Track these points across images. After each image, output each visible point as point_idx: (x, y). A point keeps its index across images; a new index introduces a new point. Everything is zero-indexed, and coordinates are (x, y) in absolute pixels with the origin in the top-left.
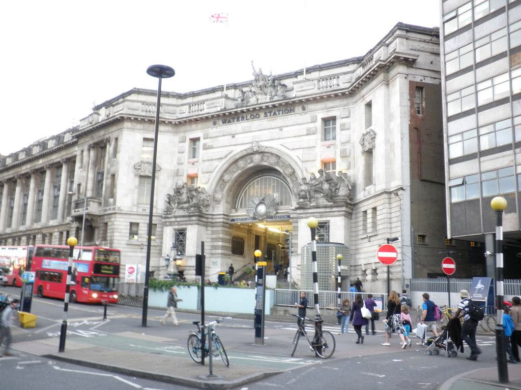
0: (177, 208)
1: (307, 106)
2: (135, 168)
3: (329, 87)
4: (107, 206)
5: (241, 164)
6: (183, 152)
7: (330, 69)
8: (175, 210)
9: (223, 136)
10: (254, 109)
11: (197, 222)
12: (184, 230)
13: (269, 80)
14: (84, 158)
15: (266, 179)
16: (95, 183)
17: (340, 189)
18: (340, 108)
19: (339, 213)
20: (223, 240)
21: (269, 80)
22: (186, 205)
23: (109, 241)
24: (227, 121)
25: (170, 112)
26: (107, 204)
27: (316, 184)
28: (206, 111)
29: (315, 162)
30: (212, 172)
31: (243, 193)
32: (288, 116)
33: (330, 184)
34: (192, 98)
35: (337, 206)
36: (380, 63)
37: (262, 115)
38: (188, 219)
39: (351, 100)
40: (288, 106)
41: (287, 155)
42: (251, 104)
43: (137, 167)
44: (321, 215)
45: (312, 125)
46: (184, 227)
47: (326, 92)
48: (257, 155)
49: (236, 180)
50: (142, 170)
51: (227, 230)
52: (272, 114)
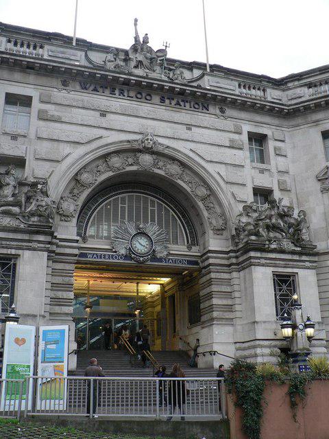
5: (116, 161)
9: (84, 108)
12: (10, 260)
15: (138, 199)
22: (16, 209)
24: (92, 88)
30: (58, 161)
31: (95, 213)
32: (200, 114)
35: (306, 254)
37: (156, 99)
38: (26, 237)
40: (200, 100)
41: (203, 167)
45: (236, 137)
46: (13, 252)
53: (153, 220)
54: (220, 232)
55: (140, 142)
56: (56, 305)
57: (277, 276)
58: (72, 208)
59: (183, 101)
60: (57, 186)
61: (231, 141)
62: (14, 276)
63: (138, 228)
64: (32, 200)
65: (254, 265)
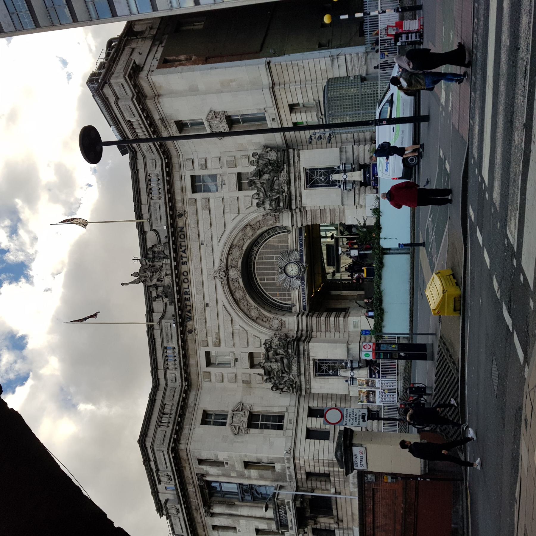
0: (289, 373)
1: (177, 212)
2: (238, 433)
3: (160, 195)
4: (285, 474)
5: (239, 294)
6: (222, 374)
7: (140, 192)
8: (291, 376)
9: (205, 319)
10: (177, 276)
11: (305, 343)
13: (146, 264)
14: (223, 524)
16: (256, 505)
17: (270, 158)
18: (182, 170)
19: (296, 156)
20: (329, 316)
21: (146, 264)
22: (285, 361)
23: (331, 469)
24: (189, 314)
25: (172, 394)
26: (281, 477)
27: (263, 191)
28: (175, 345)
29: (239, 198)
30: (247, 333)
31: (274, 298)
32: (188, 234)
33: (264, 173)
34: (159, 371)
36: (134, 99)
39: (175, 160)
42: (171, 283)
43: (236, 431)
44: (297, 178)
45: (199, 203)
46: (311, 362)
47: (164, 185)
48: (229, 273)
49: (258, 304)
50: (240, 425)
51: (316, 315)
52: (184, 255)
53: (272, 258)
54: (277, 217)
55: (222, 280)
56: (339, 328)
57: (307, 184)
58: (276, 321)
59: (181, 248)
60: (265, 334)
61: (204, 209)
62: (326, 360)
63: (281, 273)
64: (278, 352)
65: (302, 205)
